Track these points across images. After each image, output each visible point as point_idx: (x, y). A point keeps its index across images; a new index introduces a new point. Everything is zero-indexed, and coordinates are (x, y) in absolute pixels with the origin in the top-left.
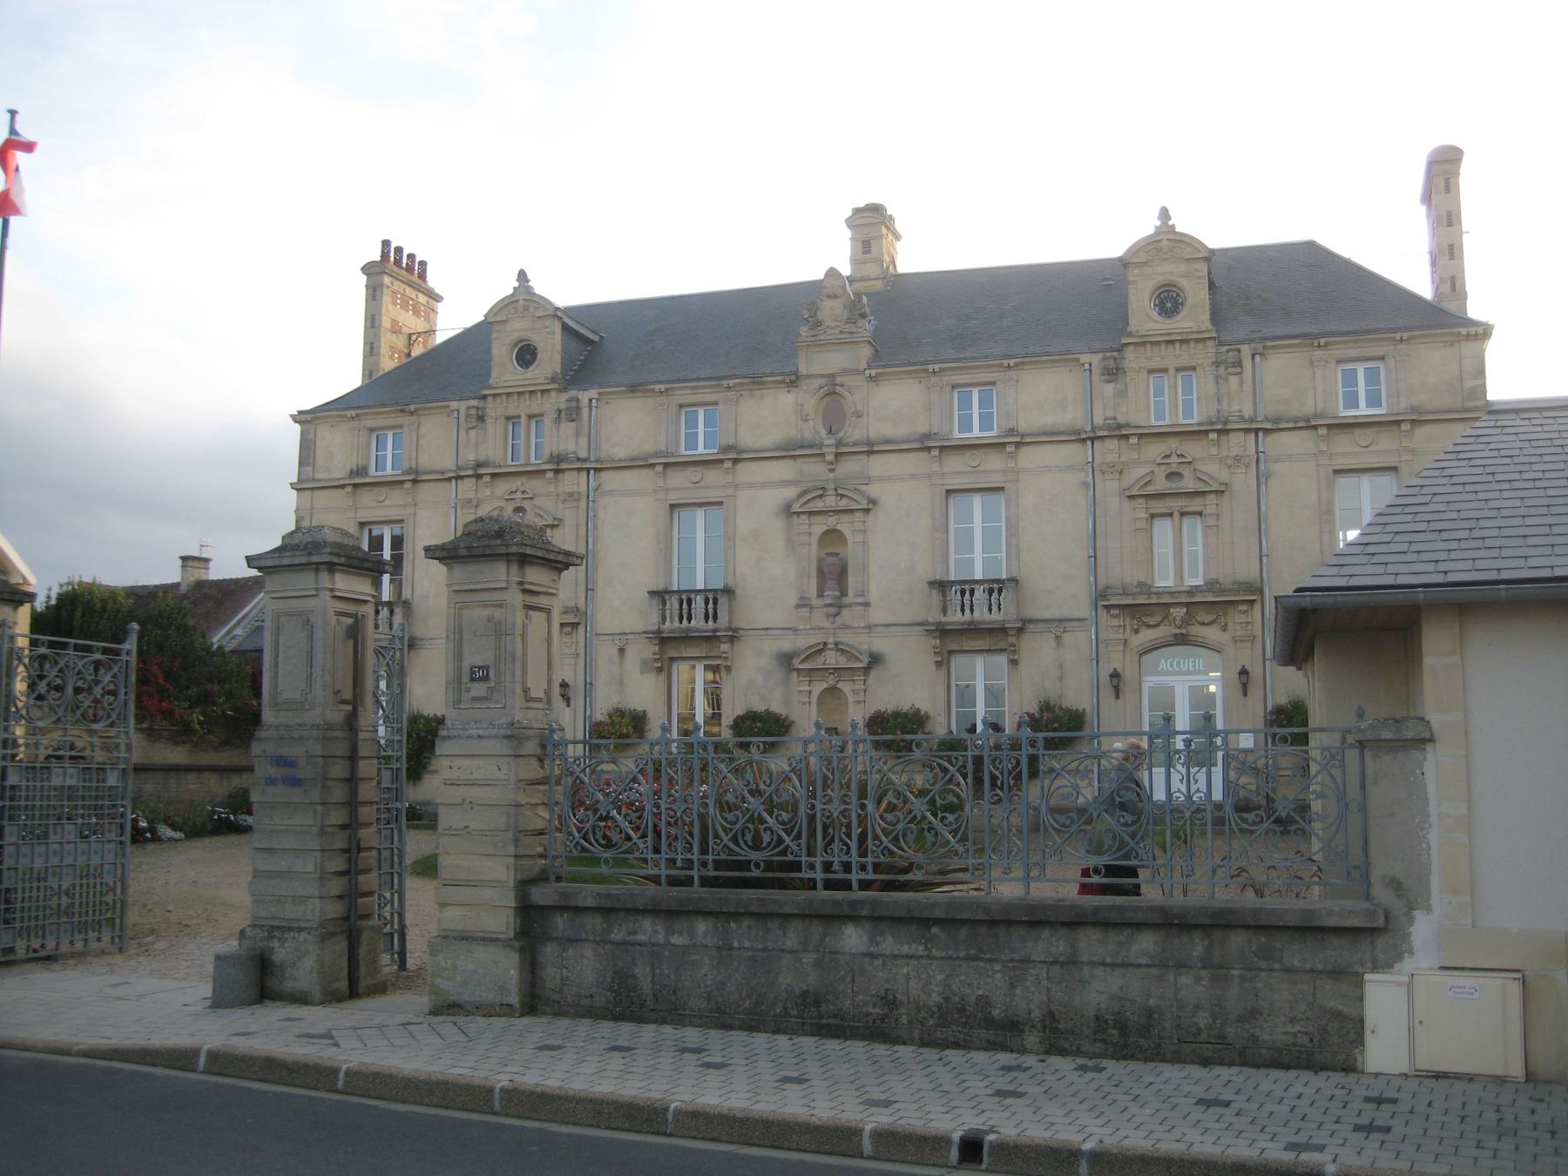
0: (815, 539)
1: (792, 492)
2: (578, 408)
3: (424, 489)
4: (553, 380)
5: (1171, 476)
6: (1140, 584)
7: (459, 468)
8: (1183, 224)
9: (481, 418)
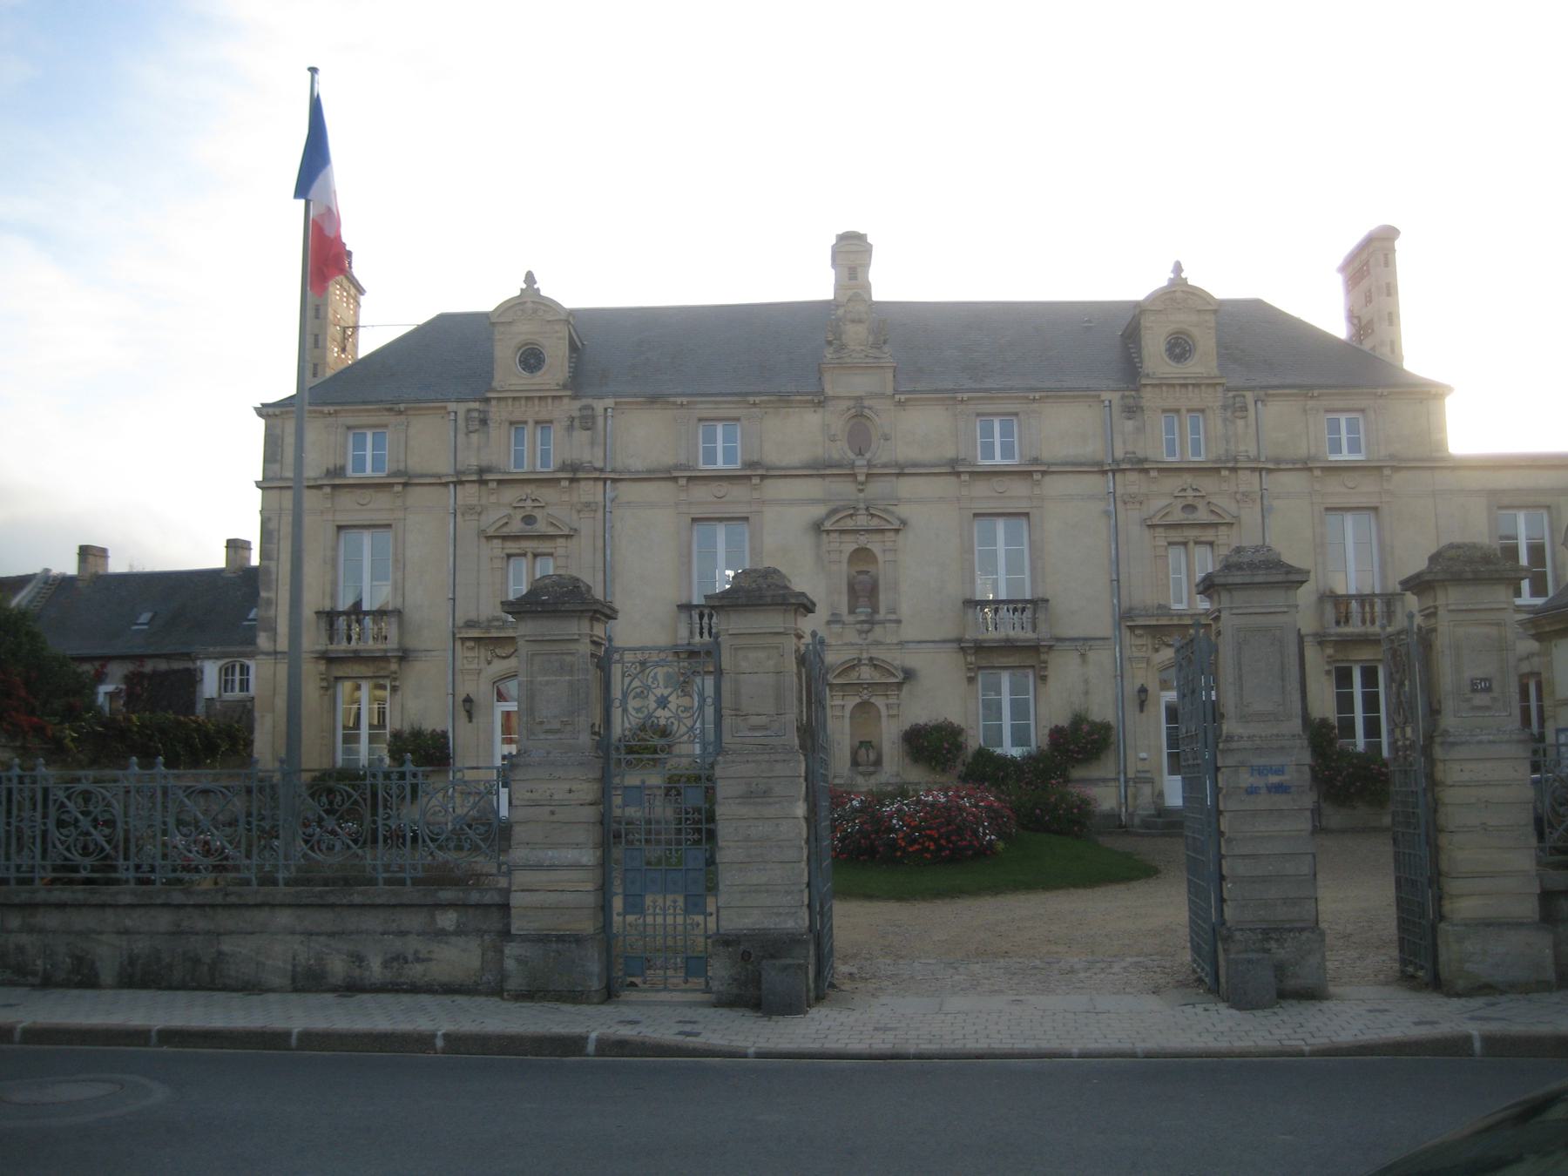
0: (845, 556)
1: (819, 511)
2: (593, 417)
3: (415, 494)
4: (565, 387)
5: (1189, 508)
6: (1160, 607)
7: (458, 473)
8: (1194, 278)
9: (484, 422)
